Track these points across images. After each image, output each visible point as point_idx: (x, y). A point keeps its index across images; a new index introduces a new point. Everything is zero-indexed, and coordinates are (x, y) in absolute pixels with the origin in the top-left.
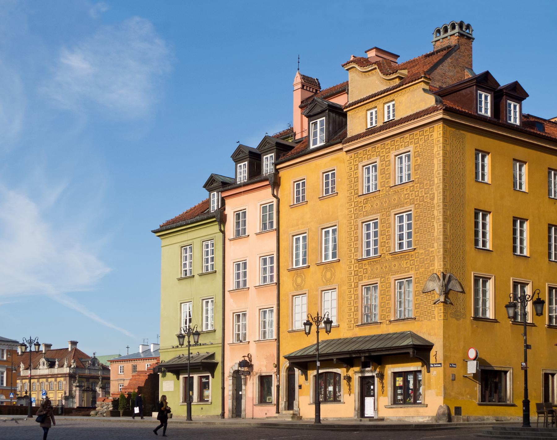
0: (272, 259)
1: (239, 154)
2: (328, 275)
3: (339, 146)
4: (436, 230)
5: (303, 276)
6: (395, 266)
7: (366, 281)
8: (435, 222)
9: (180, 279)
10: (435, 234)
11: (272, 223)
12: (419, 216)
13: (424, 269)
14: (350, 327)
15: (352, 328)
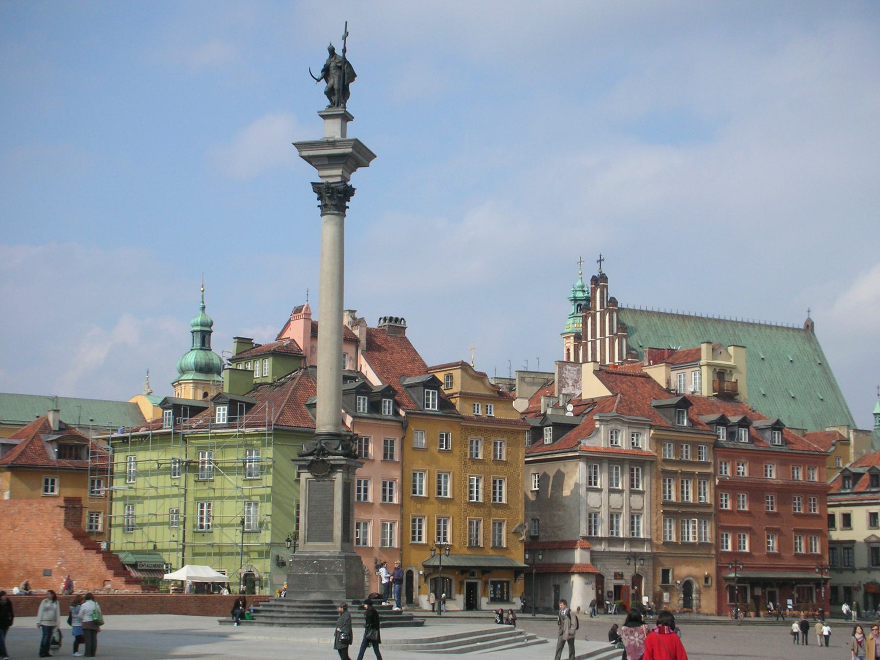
0: (391, 485)
2: (444, 507)
7: (472, 517)
11: (392, 456)
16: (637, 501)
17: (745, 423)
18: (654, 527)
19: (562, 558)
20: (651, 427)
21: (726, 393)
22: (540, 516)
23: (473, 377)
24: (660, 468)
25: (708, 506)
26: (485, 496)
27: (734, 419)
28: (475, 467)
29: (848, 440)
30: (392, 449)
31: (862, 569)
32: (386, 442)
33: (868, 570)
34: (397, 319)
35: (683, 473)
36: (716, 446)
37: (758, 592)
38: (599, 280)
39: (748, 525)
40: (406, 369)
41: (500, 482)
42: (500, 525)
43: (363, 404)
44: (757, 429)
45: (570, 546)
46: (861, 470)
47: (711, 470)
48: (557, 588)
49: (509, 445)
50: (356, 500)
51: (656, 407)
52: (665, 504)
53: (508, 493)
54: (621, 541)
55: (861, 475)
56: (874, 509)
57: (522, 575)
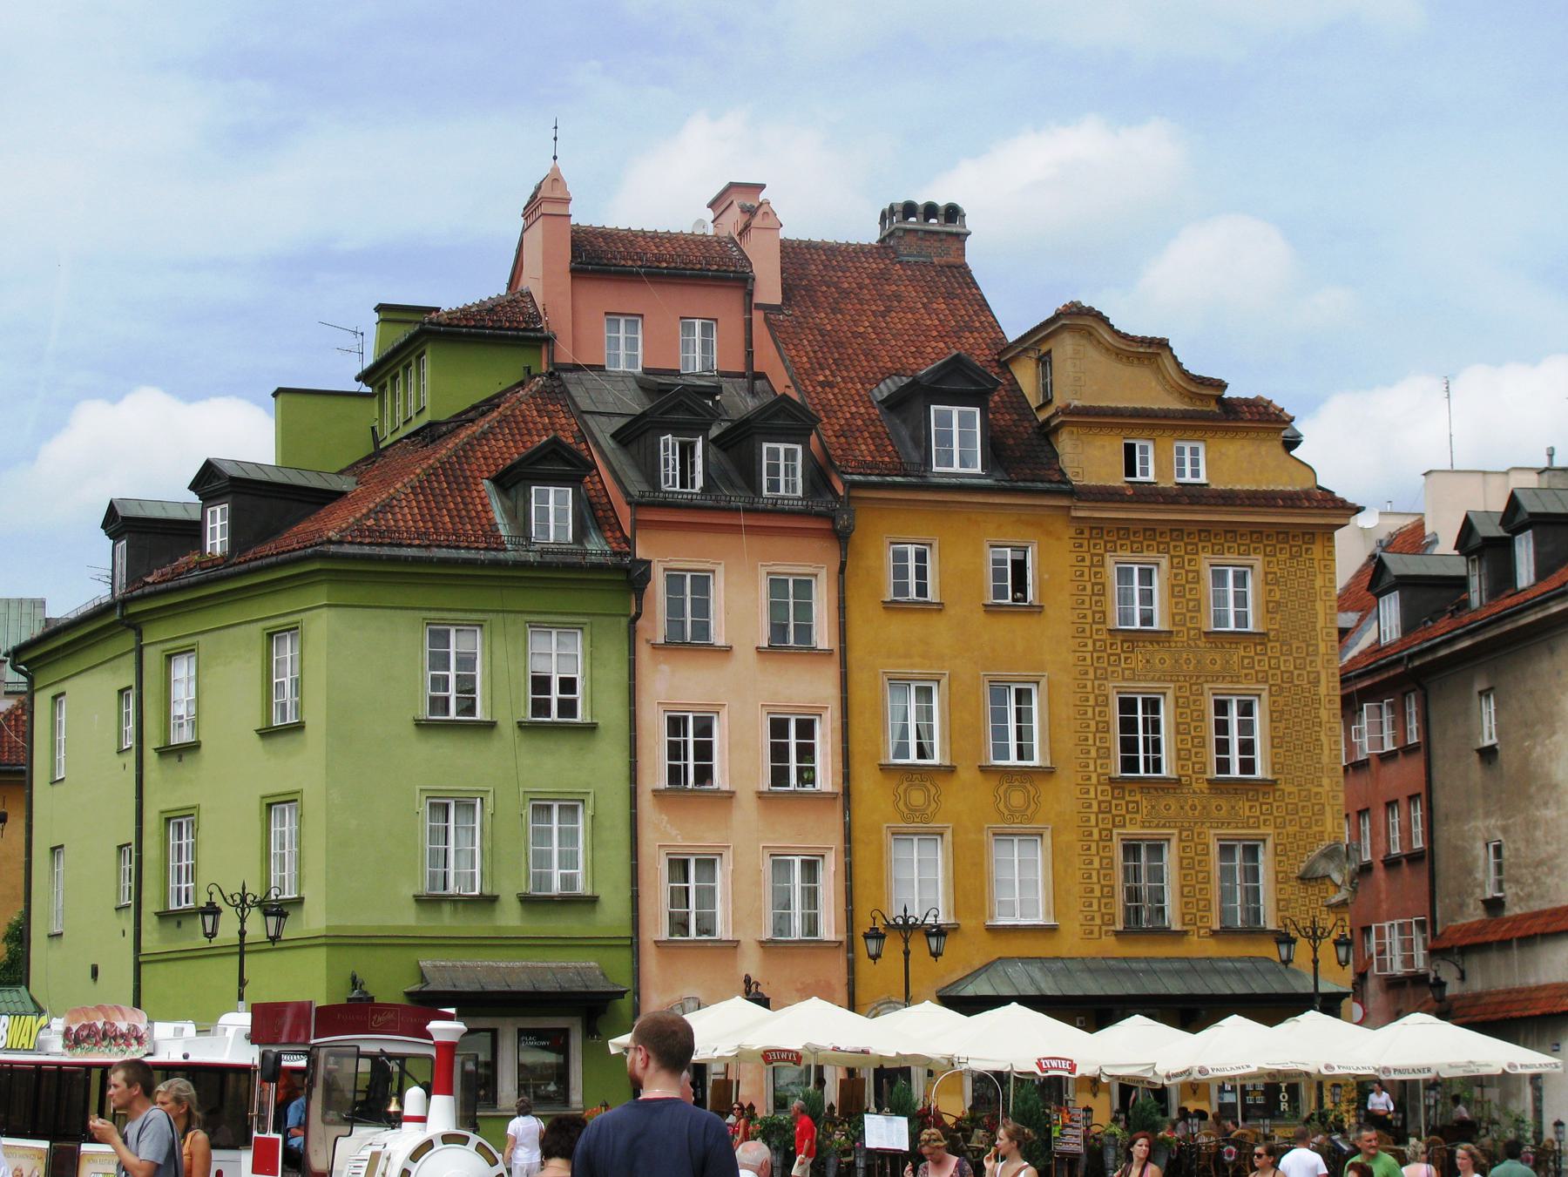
0: (806, 729)
1: (673, 409)
2: (1017, 799)
3: (1065, 502)
4: (1326, 752)
5: (933, 791)
6: (1219, 808)
7: (1133, 830)
8: (1323, 737)
9: (421, 725)
10: (1325, 759)
11: (804, 632)
12: (1282, 712)
13: (1297, 828)
14: (1091, 932)
15: (1096, 934)
22: (1505, 830)
23: (1119, 354)
26: (1180, 756)
28: (1137, 660)
30: (804, 609)
32: (777, 585)
34: (931, 210)
40: (919, 353)
41: (1246, 709)
42: (1251, 852)
43: (682, 464)
49: (1270, 580)
50: (663, 782)
53: (1275, 742)
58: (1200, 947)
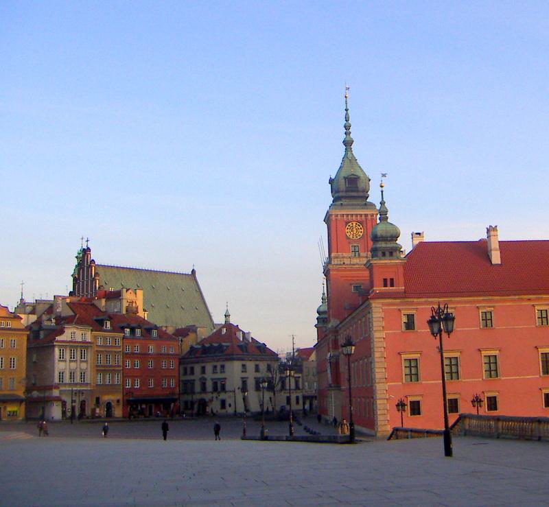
16: (84, 366)
17: (139, 327)
18: (92, 377)
19: (47, 394)
20: (92, 331)
21: (132, 311)
24: (96, 349)
25: (119, 366)
27: (133, 325)
29: (196, 332)
31: (198, 393)
33: (201, 393)
35: (106, 351)
36: (124, 338)
37: (144, 406)
38: (86, 252)
39: (138, 375)
44: (145, 329)
45: (51, 388)
46: (199, 347)
47: (121, 350)
48: (43, 408)
51: (96, 320)
52: (97, 366)
54: (76, 384)
55: (199, 349)
56: (203, 365)
57: (24, 403)
58: (7, 392)
